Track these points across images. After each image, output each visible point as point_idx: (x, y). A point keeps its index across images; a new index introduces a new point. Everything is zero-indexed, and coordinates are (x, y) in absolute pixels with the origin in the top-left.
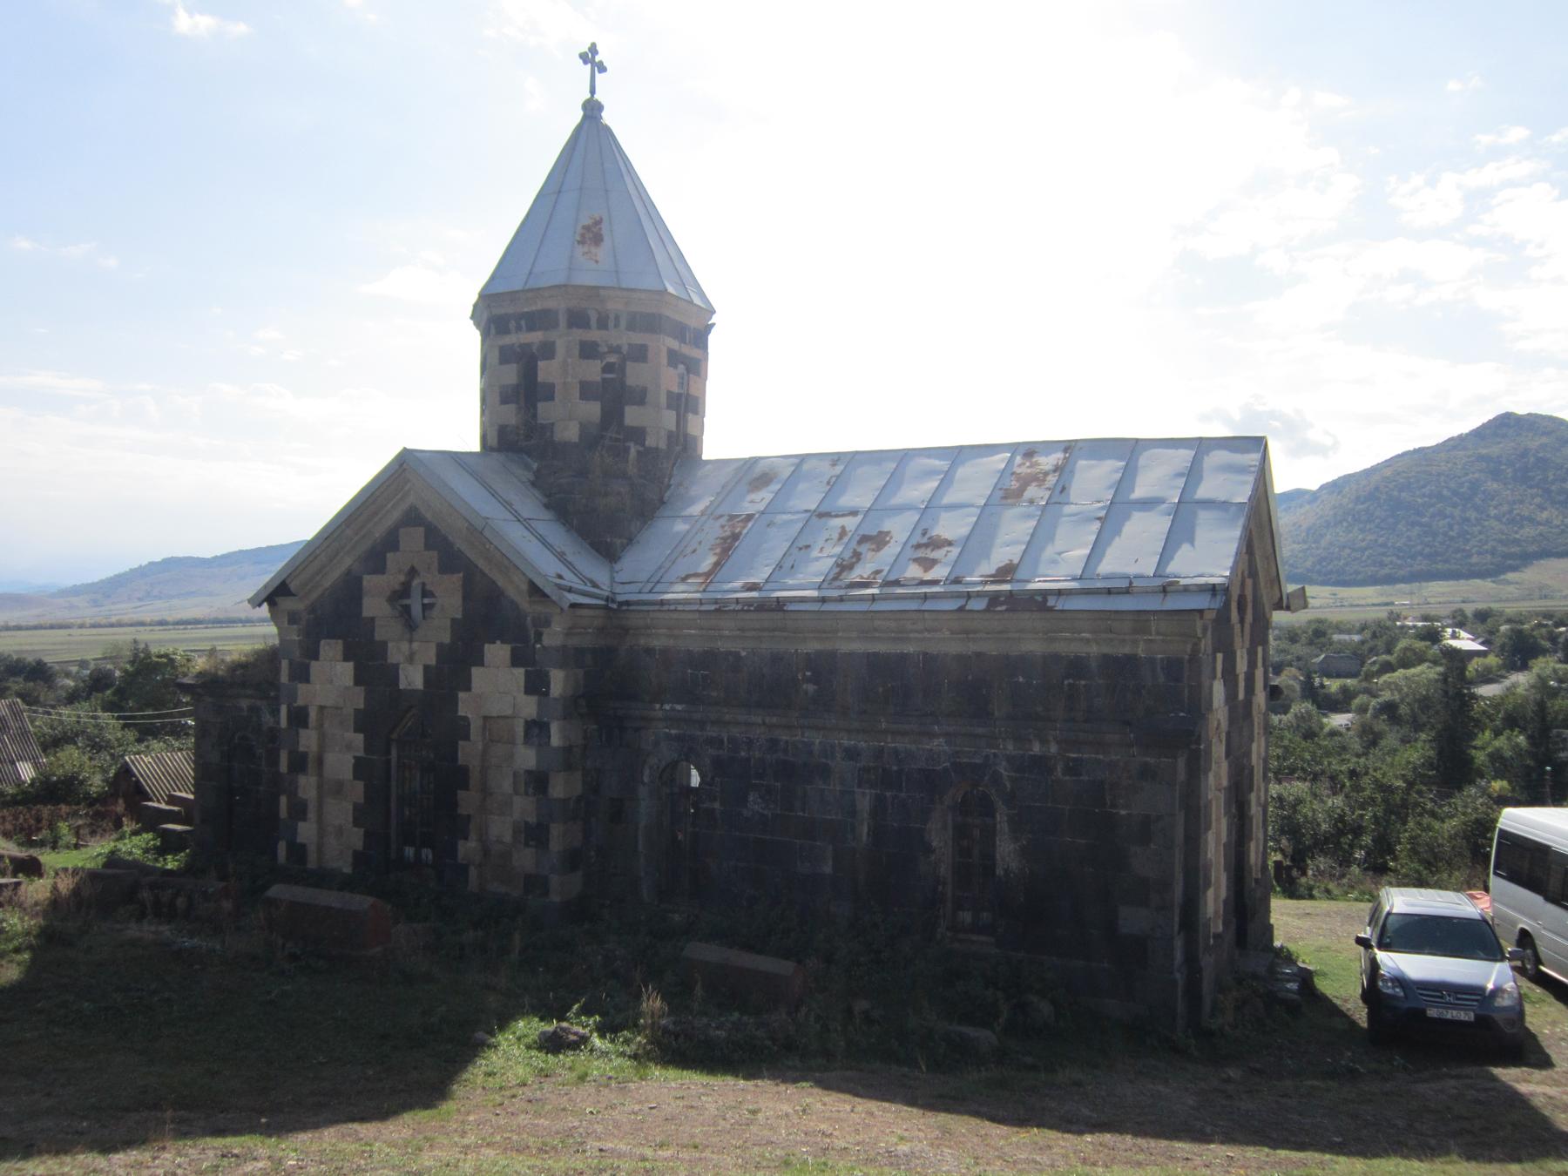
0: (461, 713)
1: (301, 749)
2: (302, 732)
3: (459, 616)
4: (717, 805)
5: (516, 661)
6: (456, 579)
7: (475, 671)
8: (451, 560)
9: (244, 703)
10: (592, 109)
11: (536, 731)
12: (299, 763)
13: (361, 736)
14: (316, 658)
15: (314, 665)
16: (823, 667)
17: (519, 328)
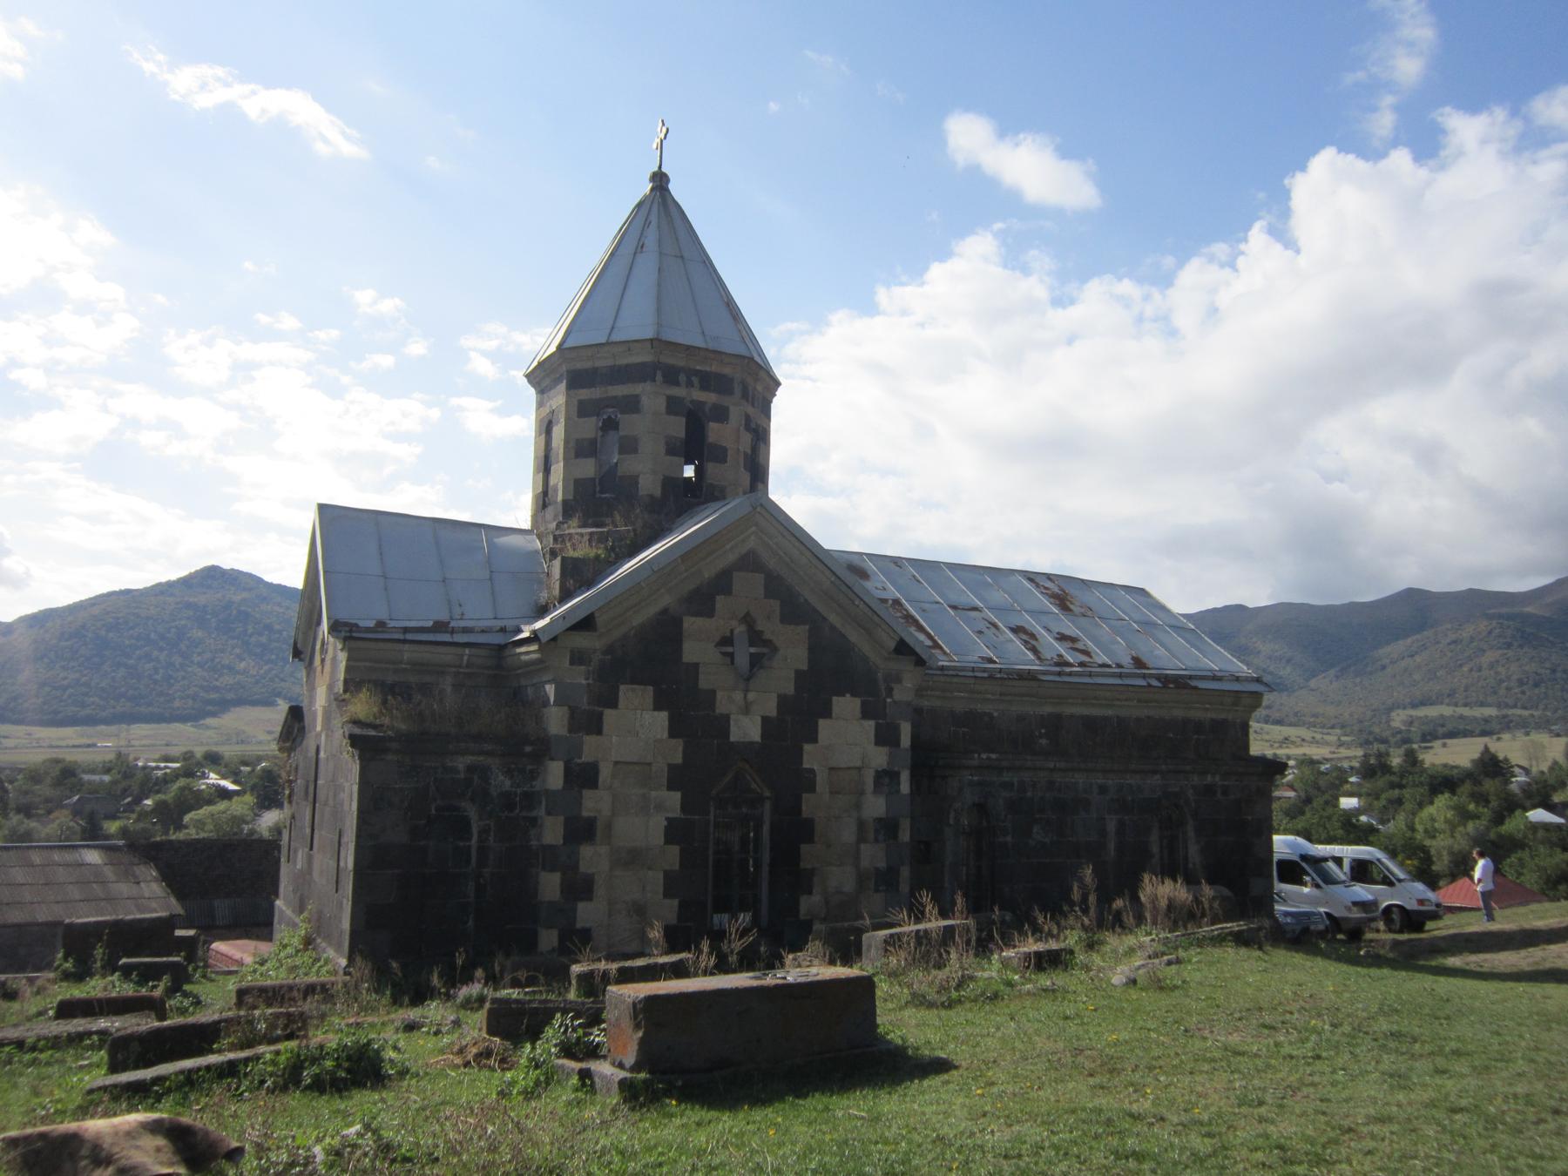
0: (806, 765)
1: (585, 814)
2: (587, 793)
3: (805, 668)
4: (1009, 839)
5: (866, 713)
6: (803, 630)
7: (822, 723)
8: (794, 610)
9: (461, 763)
10: (660, 180)
11: (887, 780)
12: (582, 831)
13: (676, 797)
14: (613, 704)
15: (609, 714)
16: (1055, 724)
17: (690, 384)
